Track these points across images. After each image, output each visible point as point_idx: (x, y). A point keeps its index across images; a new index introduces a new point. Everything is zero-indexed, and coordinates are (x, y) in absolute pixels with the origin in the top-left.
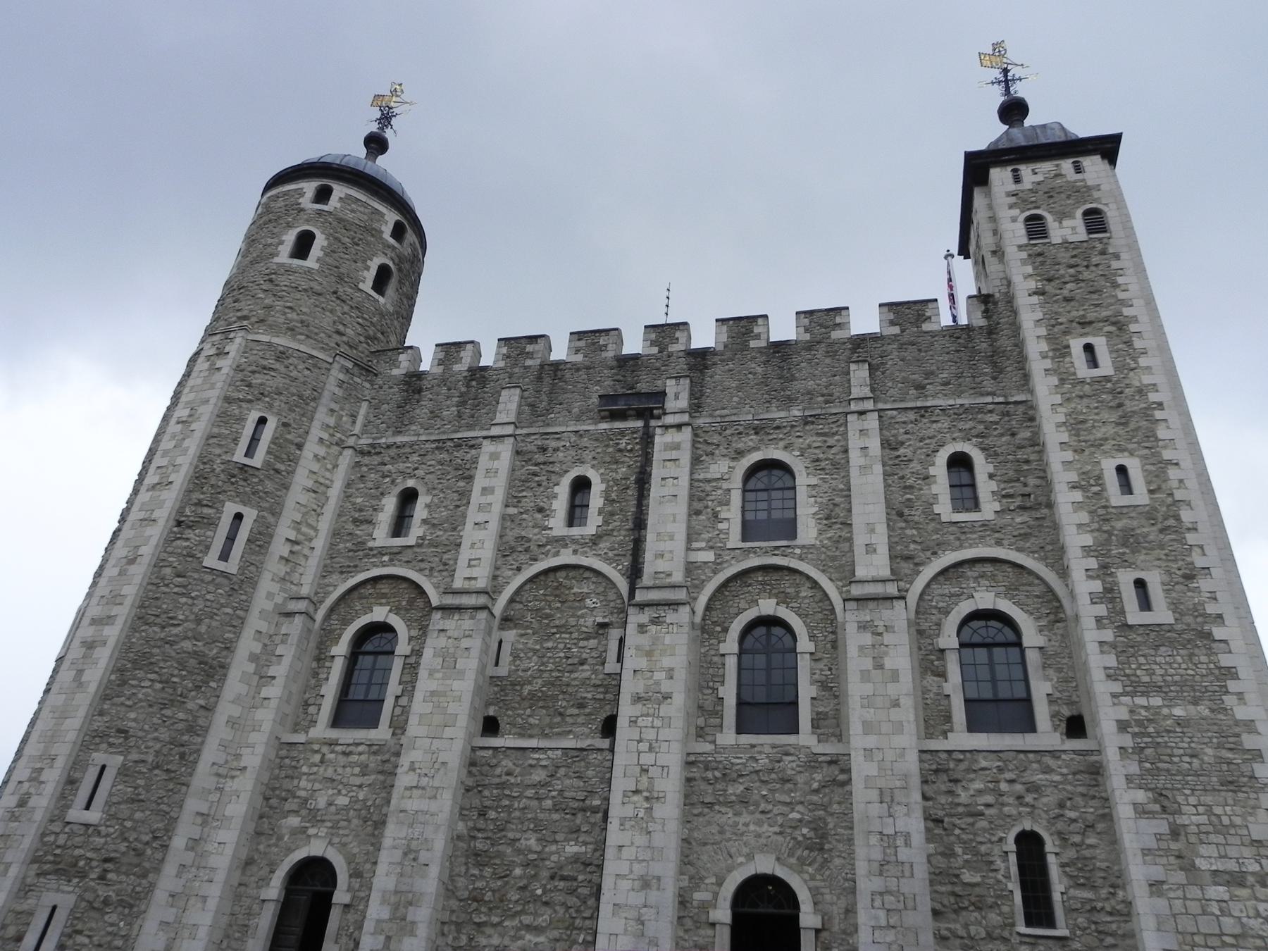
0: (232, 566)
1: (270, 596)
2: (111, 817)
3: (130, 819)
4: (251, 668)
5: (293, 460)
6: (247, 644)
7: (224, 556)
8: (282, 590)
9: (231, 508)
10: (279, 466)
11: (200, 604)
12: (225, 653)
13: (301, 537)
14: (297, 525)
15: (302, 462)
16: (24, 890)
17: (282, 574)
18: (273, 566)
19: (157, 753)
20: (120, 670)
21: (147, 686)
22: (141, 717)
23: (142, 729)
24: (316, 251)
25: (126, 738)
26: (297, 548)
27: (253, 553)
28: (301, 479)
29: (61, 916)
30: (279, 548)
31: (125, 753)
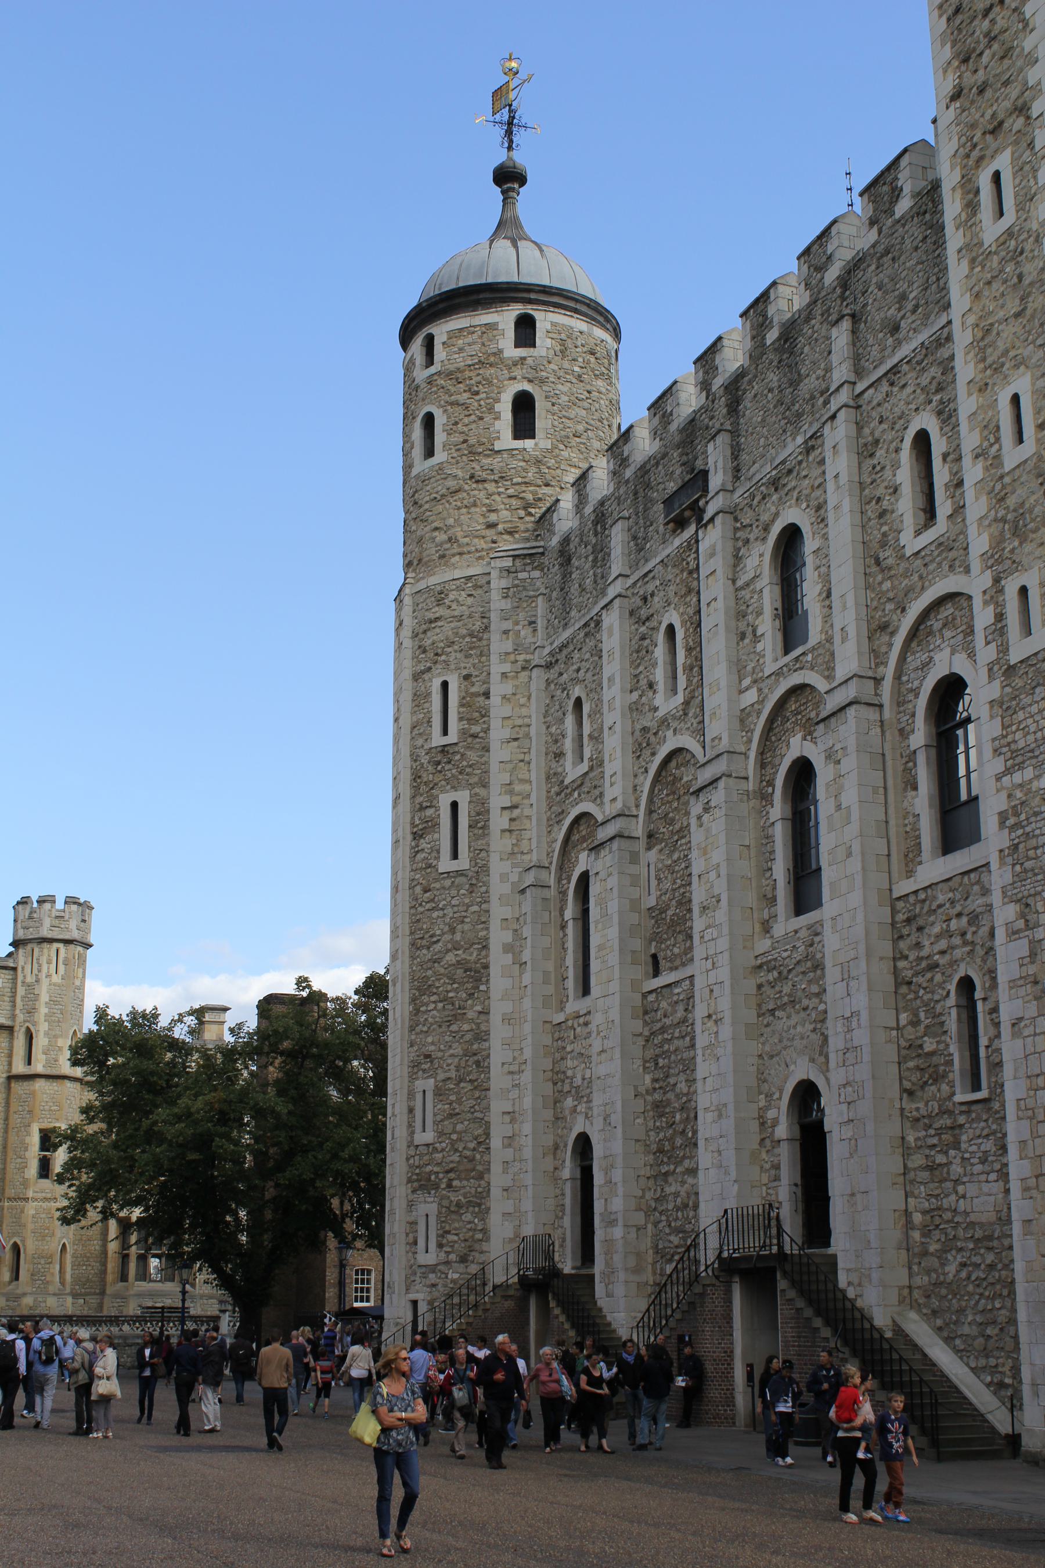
0: (464, 862)
1: (504, 877)
2: (441, 1134)
3: (454, 1132)
4: (509, 958)
5: (485, 714)
6: (498, 937)
7: (455, 856)
8: (514, 866)
9: (444, 801)
10: (476, 729)
11: (449, 911)
12: (484, 953)
13: (516, 799)
14: (508, 788)
15: (493, 713)
16: (411, 1205)
17: (509, 849)
18: (498, 844)
19: (458, 1068)
20: (413, 1000)
21: (434, 1012)
22: (436, 1039)
23: (440, 1050)
24: (440, 437)
25: (432, 1062)
26: (516, 812)
27: (478, 838)
28: (498, 733)
29: (433, 1220)
30: (498, 821)
31: (434, 1076)
